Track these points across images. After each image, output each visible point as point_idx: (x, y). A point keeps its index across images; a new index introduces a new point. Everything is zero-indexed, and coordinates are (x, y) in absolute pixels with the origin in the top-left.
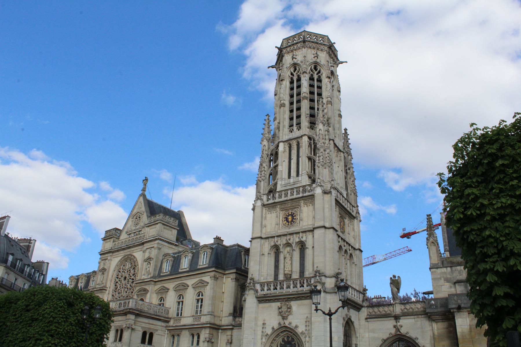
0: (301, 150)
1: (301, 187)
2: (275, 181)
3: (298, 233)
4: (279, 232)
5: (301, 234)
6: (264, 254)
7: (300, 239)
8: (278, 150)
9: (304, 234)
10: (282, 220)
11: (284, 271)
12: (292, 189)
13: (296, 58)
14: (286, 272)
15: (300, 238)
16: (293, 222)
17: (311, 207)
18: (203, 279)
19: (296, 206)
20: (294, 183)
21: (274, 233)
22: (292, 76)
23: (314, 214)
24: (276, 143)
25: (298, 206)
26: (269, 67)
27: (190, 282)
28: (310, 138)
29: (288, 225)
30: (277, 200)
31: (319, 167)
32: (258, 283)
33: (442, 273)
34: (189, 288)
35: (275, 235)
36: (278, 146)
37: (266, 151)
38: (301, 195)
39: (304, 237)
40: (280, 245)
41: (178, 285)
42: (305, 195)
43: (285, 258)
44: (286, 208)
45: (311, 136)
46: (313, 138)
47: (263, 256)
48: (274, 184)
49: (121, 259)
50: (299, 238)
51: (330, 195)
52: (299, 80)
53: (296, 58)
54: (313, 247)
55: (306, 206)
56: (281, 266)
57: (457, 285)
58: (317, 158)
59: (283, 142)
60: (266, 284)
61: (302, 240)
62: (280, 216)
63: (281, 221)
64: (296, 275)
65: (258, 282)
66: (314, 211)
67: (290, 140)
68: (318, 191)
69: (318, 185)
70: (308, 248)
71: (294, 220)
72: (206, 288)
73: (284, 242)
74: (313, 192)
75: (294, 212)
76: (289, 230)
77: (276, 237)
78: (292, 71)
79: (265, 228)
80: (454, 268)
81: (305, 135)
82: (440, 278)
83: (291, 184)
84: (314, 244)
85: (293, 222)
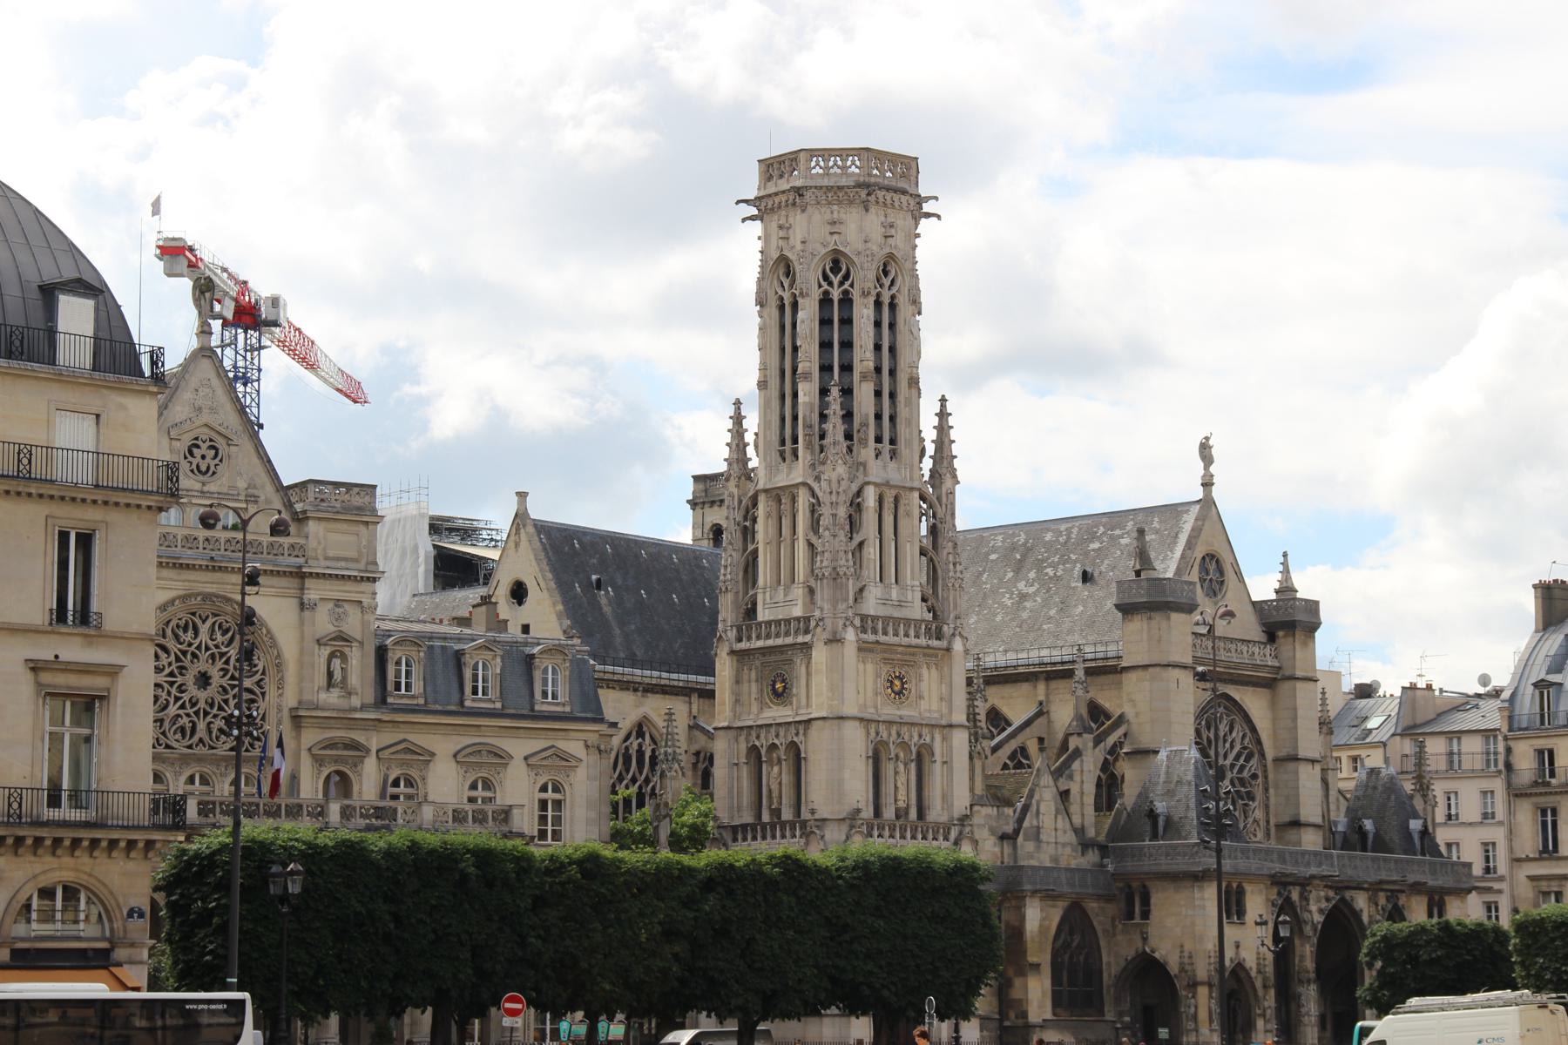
11: (896, 800)
14: (901, 804)
18: (561, 744)
24: (861, 479)
27: (518, 748)
30: (882, 638)
33: (988, 816)
34: (513, 763)
38: (923, 641)
41: (476, 750)
43: (896, 773)
49: (172, 602)
57: (1005, 842)
58: (951, 566)
64: (913, 814)
67: (887, 484)
72: (572, 775)
76: (898, 713)
80: (1000, 809)
82: (984, 826)
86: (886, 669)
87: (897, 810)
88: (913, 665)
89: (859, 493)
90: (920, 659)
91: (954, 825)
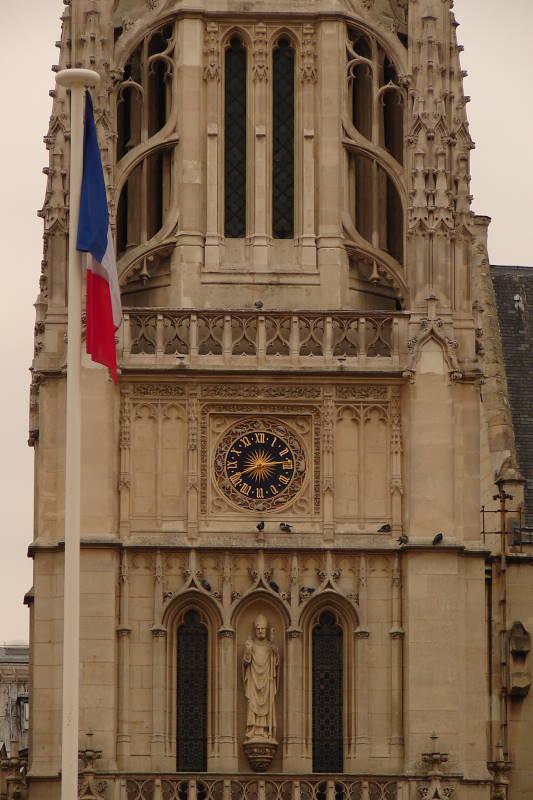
0: (303, 96)
1: (329, 319)
2: (163, 237)
3: (319, 553)
4: (203, 528)
5: (329, 558)
6: (129, 631)
7: (329, 585)
8: (171, 55)
9: (345, 565)
10: (217, 467)
11: (243, 727)
12: (280, 317)
14: (257, 737)
15: (329, 578)
16: (280, 489)
17: (377, 433)
19: (293, 408)
20: (274, 279)
21: (179, 526)
23: (396, 471)
25: (308, 413)
28: (360, 39)
29: (252, 495)
31: (431, 235)
35: (189, 545)
37: (103, 42)
38: (328, 361)
39: (342, 573)
40: (221, 597)
42: (352, 363)
43: (244, 666)
44: (242, 407)
45: (368, 32)
46: (380, 48)
47: (125, 639)
48: (156, 255)
50: (320, 577)
51: (472, 387)
54: (400, 637)
55: (347, 417)
56: (224, 700)
58: (420, 184)
59: (204, 17)
60: (158, 782)
61: (337, 589)
62: (204, 442)
63: (211, 471)
64: (299, 759)
65: (113, 768)
66: (397, 459)
68: (431, 363)
69: (432, 332)
70: (365, 635)
71: (281, 477)
74: (396, 358)
75: (280, 435)
77: (193, 555)
79: (124, 495)
81: (336, 17)
83: (259, 279)
84: (401, 623)
85: (280, 489)
86: (217, 433)
87: (246, 751)
88: (310, 413)
89: (162, 36)
90: (329, 401)
91: (406, 779)
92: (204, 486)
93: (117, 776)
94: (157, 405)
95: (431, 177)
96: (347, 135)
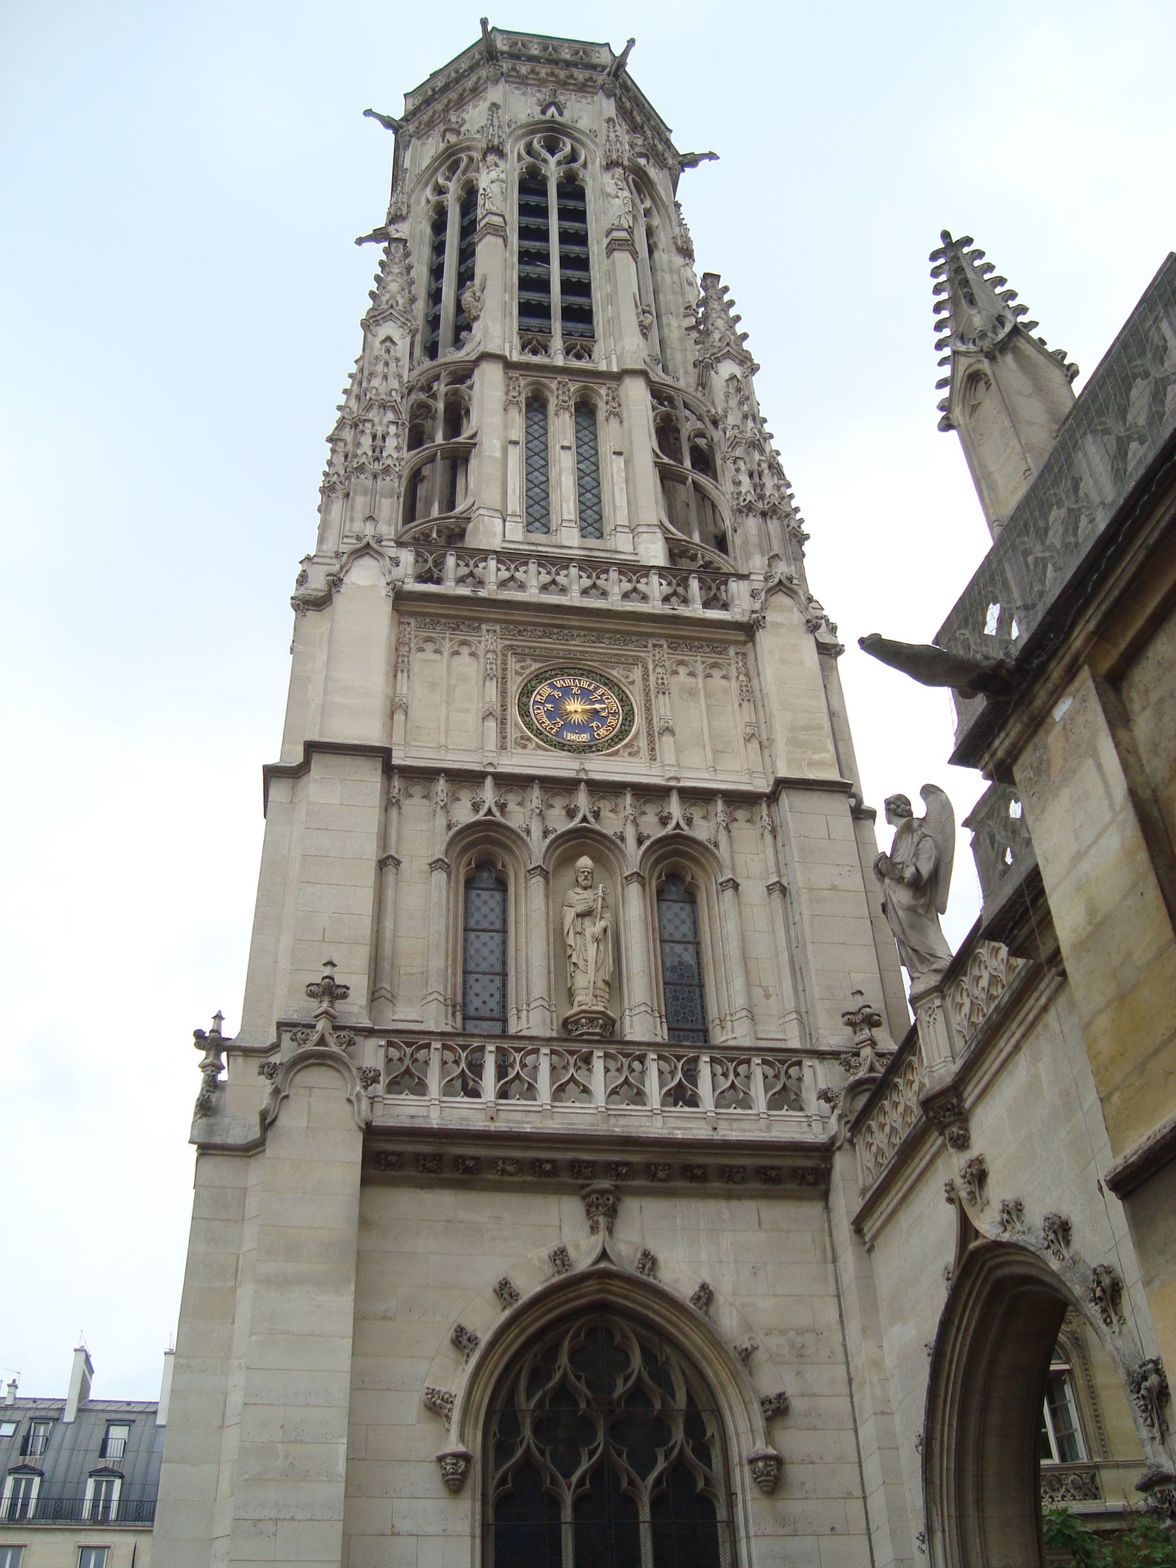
8: (471, 387)
13: (561, 114)
14: (586, 999)
22: (529, 159)
26: (369, 113)
32: (370, 1032)
36: (463, 374)
42: (683, 611)
47: (391, 869)
52: (572, 189)
53: (561, 114)
59: (509, 365)
61: (687, 831)
73: (560, 823)
77: (489, 782)
78: (535, 144)
79: (399, 717)
81: (643, 373)
92: (503, 722)
93: (370, 1032)
94: (444, 639)
95: (756, 475)
96: (657, 456)
